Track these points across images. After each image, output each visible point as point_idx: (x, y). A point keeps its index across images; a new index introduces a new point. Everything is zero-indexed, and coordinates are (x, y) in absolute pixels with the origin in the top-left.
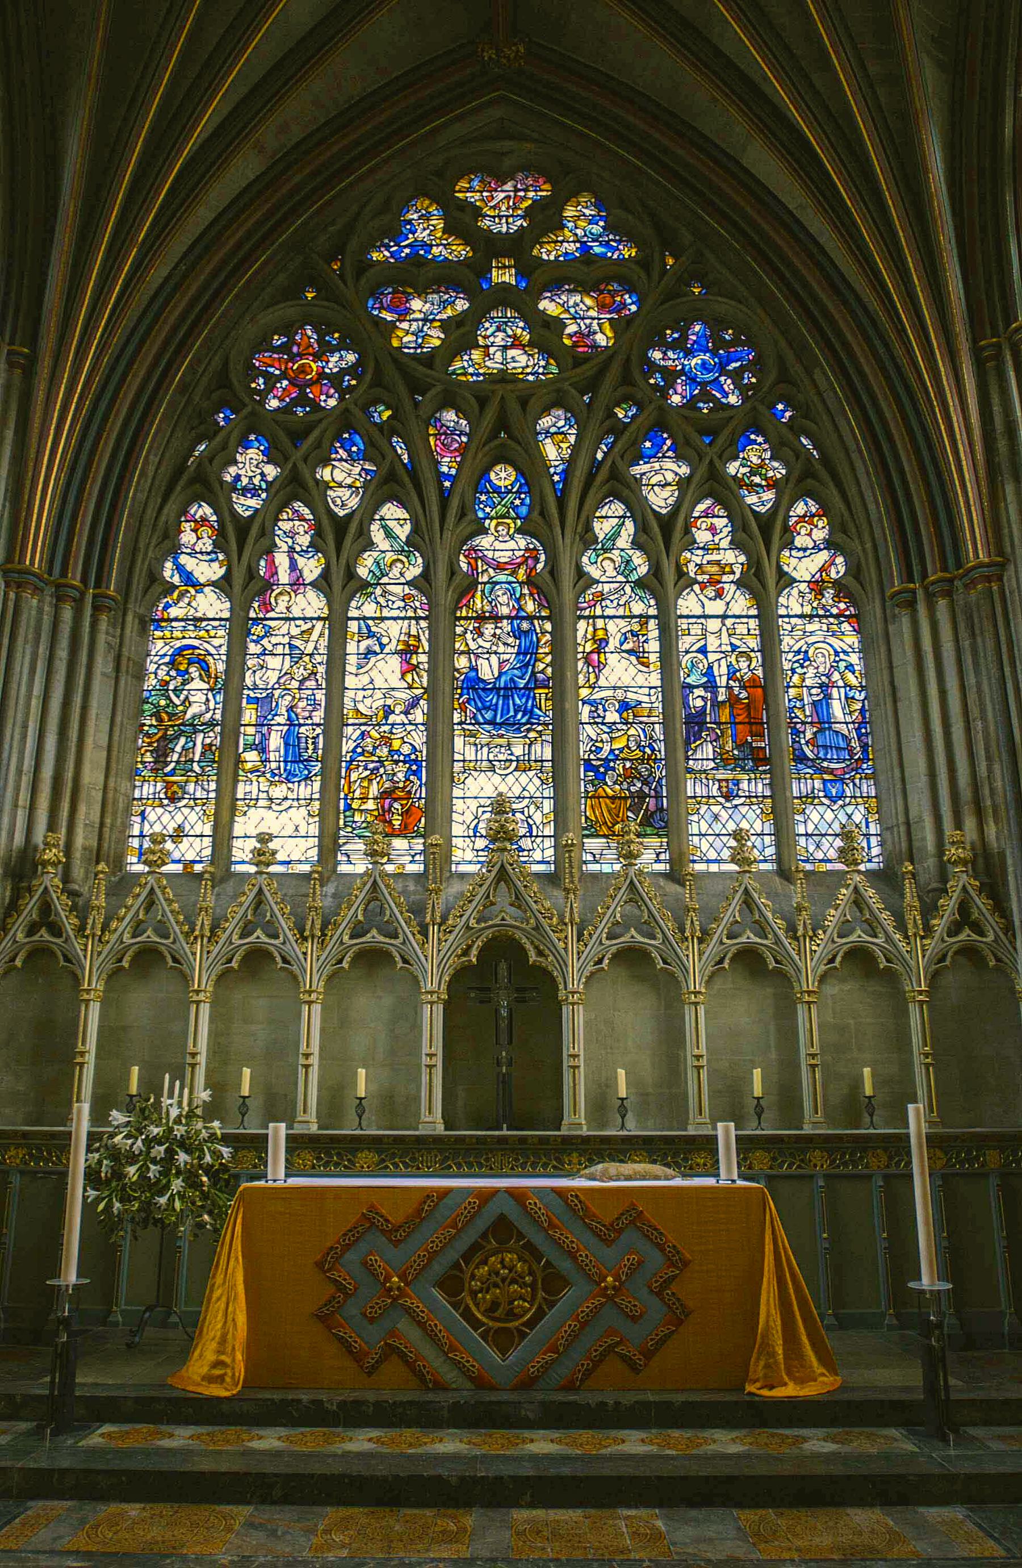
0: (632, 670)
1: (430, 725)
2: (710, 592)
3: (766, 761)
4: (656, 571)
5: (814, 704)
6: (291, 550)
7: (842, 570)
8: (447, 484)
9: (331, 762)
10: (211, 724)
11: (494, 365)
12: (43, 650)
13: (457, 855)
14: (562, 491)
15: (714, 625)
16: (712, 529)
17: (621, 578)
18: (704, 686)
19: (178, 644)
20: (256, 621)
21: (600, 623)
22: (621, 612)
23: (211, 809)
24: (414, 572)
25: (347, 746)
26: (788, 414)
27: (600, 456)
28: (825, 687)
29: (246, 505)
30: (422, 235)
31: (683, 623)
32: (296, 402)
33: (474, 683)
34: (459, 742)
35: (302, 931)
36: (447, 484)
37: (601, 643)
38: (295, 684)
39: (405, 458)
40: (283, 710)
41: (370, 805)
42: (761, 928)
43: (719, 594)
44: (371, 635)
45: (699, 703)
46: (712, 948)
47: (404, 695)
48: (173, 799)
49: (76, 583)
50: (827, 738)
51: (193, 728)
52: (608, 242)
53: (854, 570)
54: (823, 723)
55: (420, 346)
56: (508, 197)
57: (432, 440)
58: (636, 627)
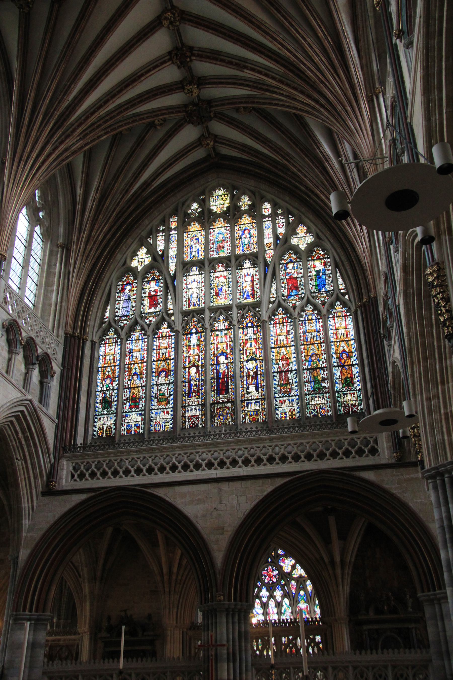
24: (290, 610)
29: (265, 600)
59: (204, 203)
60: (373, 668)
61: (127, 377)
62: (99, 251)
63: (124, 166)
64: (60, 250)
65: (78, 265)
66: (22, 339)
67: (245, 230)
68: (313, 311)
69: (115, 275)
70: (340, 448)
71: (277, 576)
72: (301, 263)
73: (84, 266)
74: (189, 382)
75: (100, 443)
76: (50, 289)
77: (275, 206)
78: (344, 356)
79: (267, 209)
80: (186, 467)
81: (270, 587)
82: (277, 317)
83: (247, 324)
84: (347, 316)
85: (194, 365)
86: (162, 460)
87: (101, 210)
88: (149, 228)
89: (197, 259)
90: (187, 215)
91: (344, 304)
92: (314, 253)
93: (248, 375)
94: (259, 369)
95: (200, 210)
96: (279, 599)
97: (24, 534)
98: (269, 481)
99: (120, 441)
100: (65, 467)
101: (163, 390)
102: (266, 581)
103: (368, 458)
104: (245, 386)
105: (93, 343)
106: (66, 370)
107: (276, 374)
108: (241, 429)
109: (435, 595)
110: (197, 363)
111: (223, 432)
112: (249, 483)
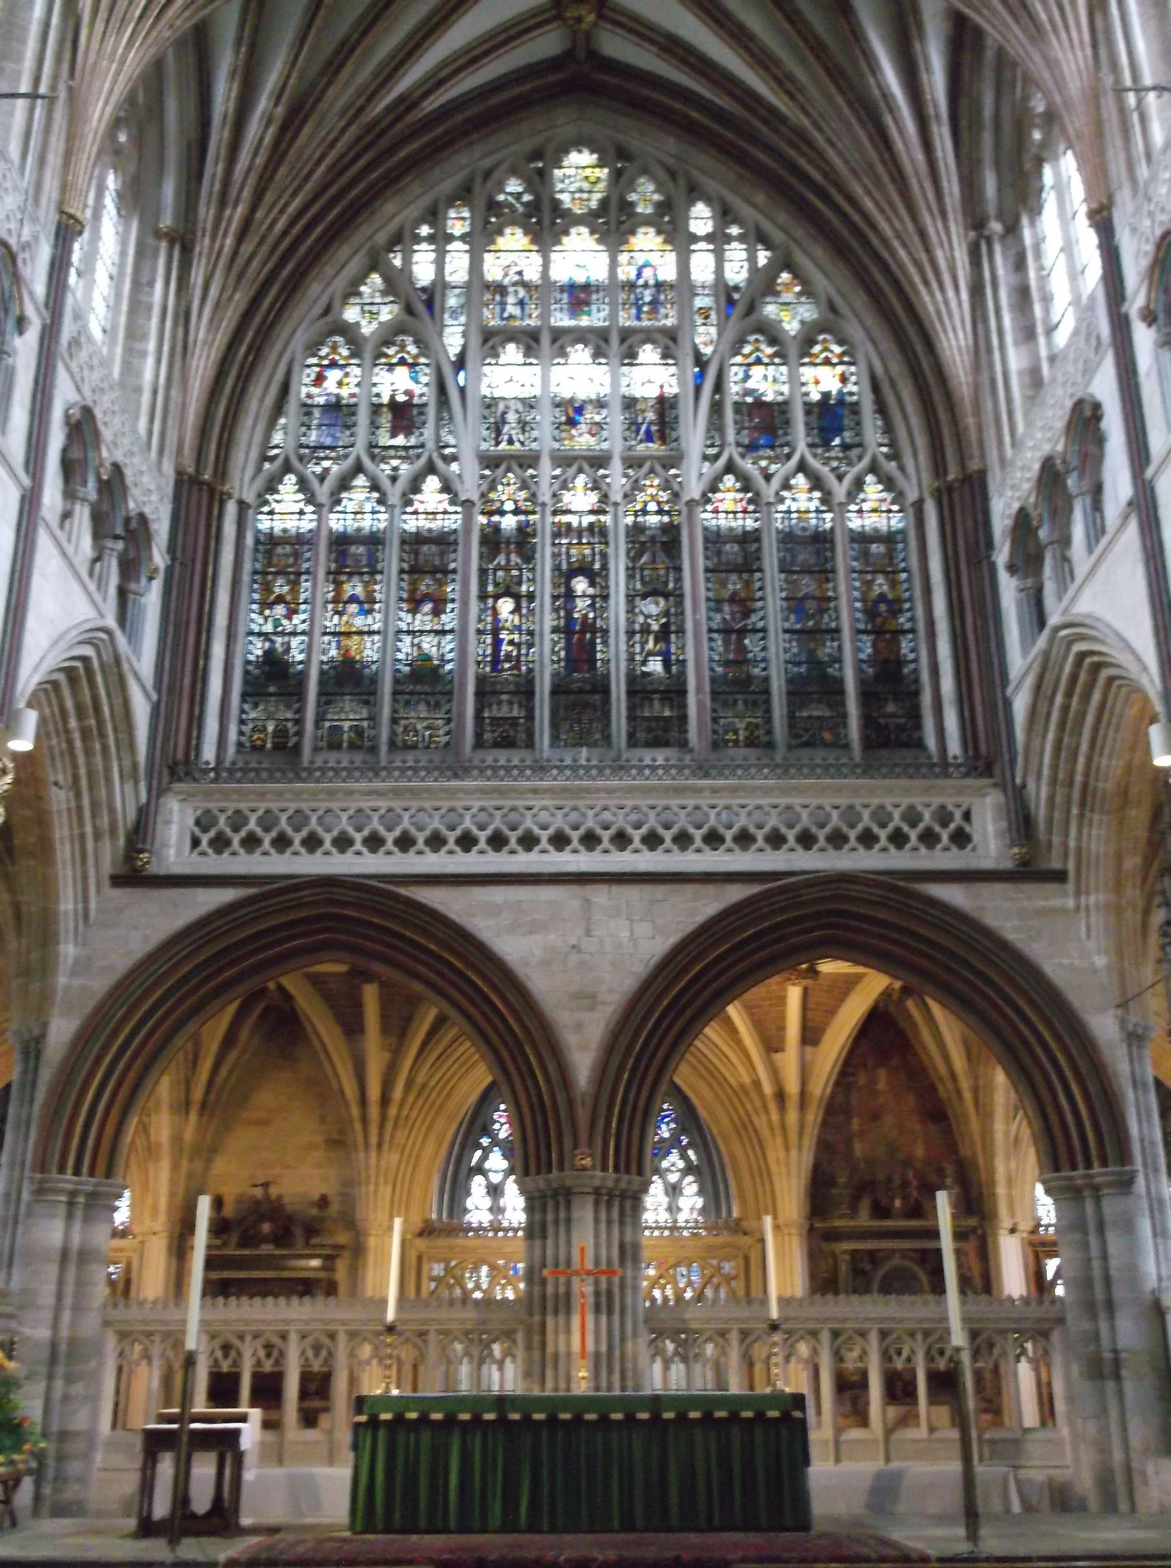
29: (495, 1178)
59: (540, 181)
60: (927, 1334)
61: (330, 606)
62: (270, 266)
63: (358, 42)
64: (164, 245)
65: (214, 292)
66: (101, 465)
67: (644, 266)
68: (811, 490)
69: (300, 339)
70: (883, 825)
72: (784, 369)
73: (231, 298)
74: (495, 632)
75: (260, 763)
76: (138, 346)
77: (725, 215)
78: (883, 607)
79: (701, 219)
80: (497, 842)
82: (719, 496)
83: (646, 503)
84: (889, 511)
85: (508, 593)
86: (437, 818)
87: (285, 153)
88: (393, 227)
89: (517, 323)
90: (493, 207)
91: (888, 483)
92: (817, 349)
93: (646, 630)
94: (673, 620)
95: (527, 198)
97: (62, 980)
98: (710, 889)
99: (312, 762)
100: (176, 817)
101: (425, 646)
103: (948, 854)
104: (638, 658)
105: (242, 505)
106: (177, 566)
107: (715, 635)
108: (628, 761)
109: (1088, 1176)
110: (514, 589)
111: (584, 763)
112: (659, 891)
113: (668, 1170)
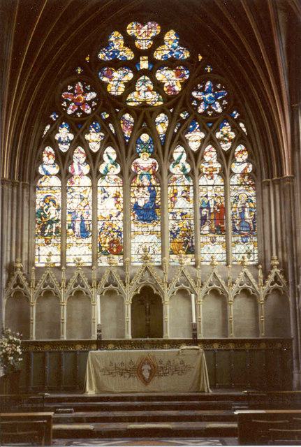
0: (185, 203)
1: (124, 220)
2: (209, 177)
3: (224, 231)
4: (192, 171)
5: (240, 213)
6: (79, 163)
7: (251, 169)
8: (127, 141)
9: (95, 232)
10: (58, 221)
11: (142, 98)
12: (10, 202)
13: (133, 260)
14: (164, 143)
15: (210, 188)
16: (211, 156)
17: (182, 173)
18: (207, 208)
19: (46, 195)
20: (69, 187)
21: (175, 188)
22: (182, 184)
23: (59, 246)
24: (118, 170)
25: (99, 227)
26: (237, 115)
27: (176, 131)
28: (243, 208)
29: (64, 148)
30: (116, 47)
31: (201, 188)
32: (76, 112)
33: (136, 207)
34: (132, 225)
35: (91, 285)
36: (127, 141)
37: (175, 194)
38: (82, 208)
39: (114, 132)
40: (79, 216)
41: (107, 245)
42: (219, 283)
43: (212, 178)
44: (105, 192)
45: (205, 213)
46: (204, 289)
47: (116, 211)
48: (48, 244)
49: (17, 181)
50: (243, 224)
51: (51, 222)
52: (179, 50)
53: (254, 171)
54: (243, 219)
55: (117, 91)
56: (145, 32)
57: (122, 125)
58: (186, 189)
71: (94, 104)
81: (77, 123)
96: (95, 147)
102: (69, 112)
113: (221, 140)
